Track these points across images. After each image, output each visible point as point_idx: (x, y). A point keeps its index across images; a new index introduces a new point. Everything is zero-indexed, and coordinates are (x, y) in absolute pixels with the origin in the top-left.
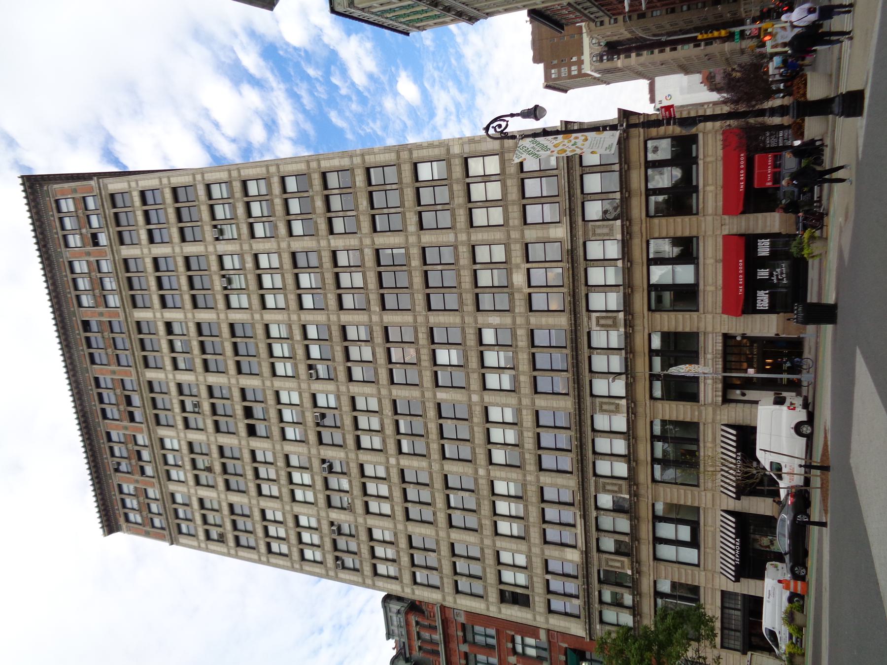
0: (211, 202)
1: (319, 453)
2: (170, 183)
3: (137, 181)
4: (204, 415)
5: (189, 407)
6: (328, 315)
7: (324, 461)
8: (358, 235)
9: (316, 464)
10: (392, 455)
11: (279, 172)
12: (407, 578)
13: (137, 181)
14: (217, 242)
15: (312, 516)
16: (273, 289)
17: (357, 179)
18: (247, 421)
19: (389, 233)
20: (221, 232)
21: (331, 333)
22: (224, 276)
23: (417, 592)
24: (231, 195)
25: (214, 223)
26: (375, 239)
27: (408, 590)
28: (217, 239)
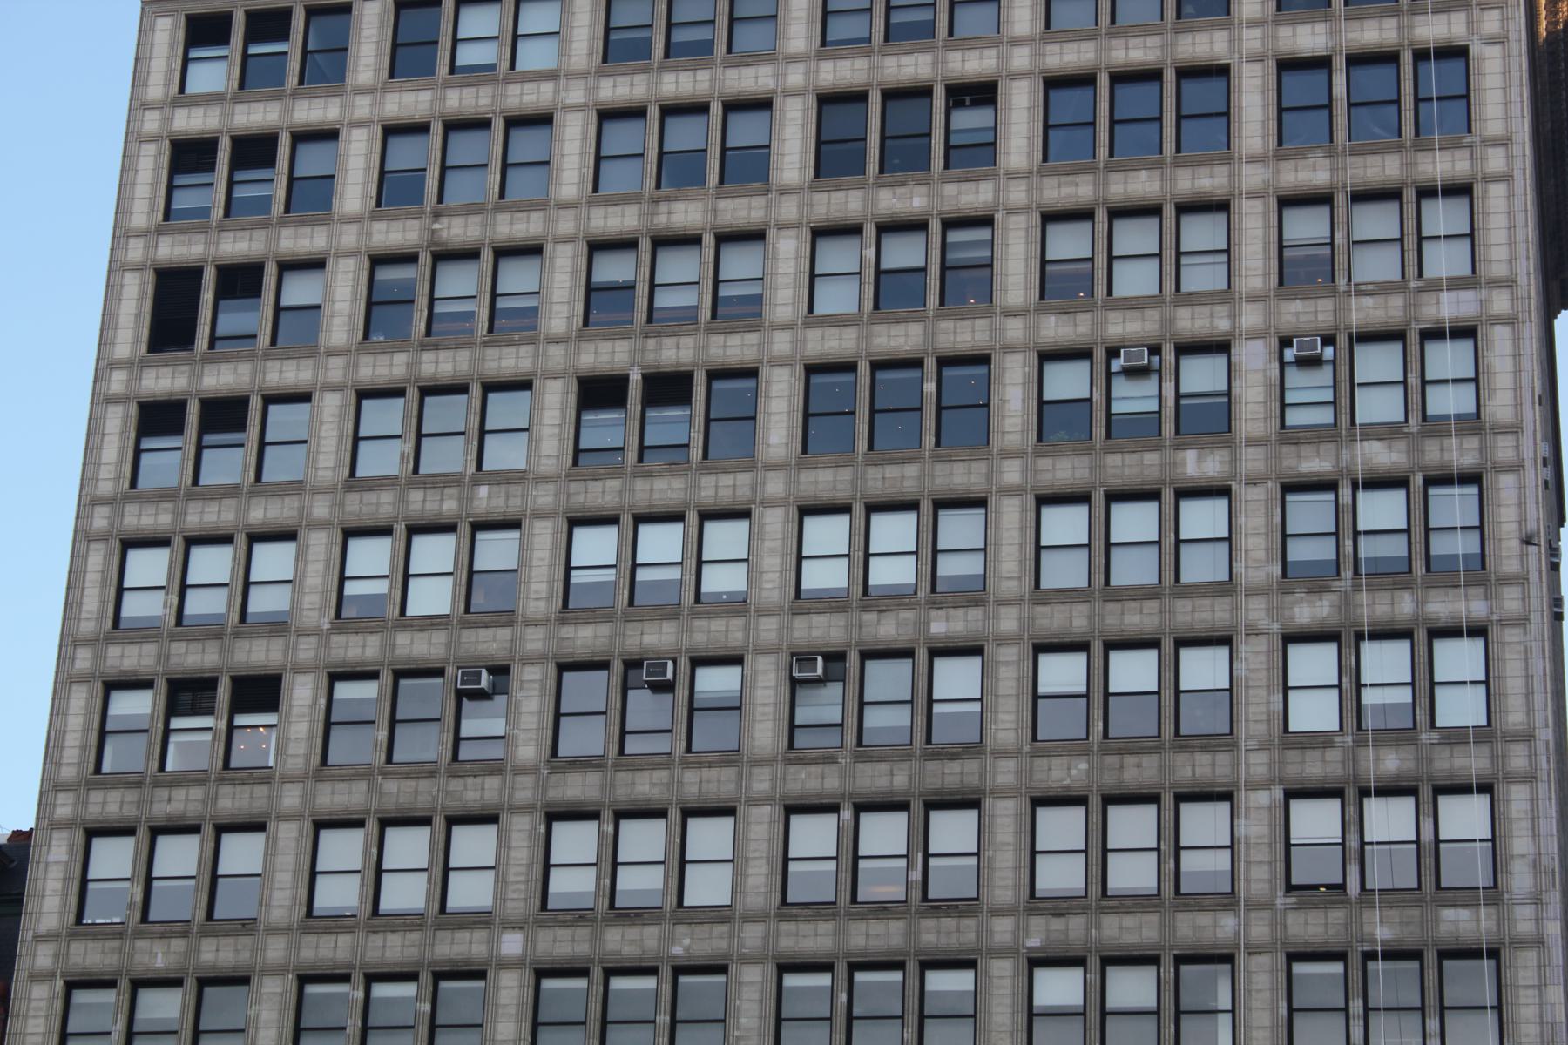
0: (1413, 338)
1: (528, 661)
2: (1488, 179)
3: (1500, 40)
4: (656, 201)
5: (684, 135)
6: (1017, 754)
7: (501, 671)
8: (1281, 900)
9: (489, 643)
10: (530, 942)
11: (1502, 623)
12: (91, 957)
13: (1500, 40)
14: (1274, 343)
15: (295, 602)
16: (1108, 545)
17: (1464, 914)
18: (635, 377)
19: (1283, 1011)
20: (1309, 362)
21: (953, 757)
22: (1155, 350)
23: (40, 992)
24: (1434, 426)
25: (1342, 340)
26: (1264, 960)
27: (44, 957)
28: (1285, 342)
